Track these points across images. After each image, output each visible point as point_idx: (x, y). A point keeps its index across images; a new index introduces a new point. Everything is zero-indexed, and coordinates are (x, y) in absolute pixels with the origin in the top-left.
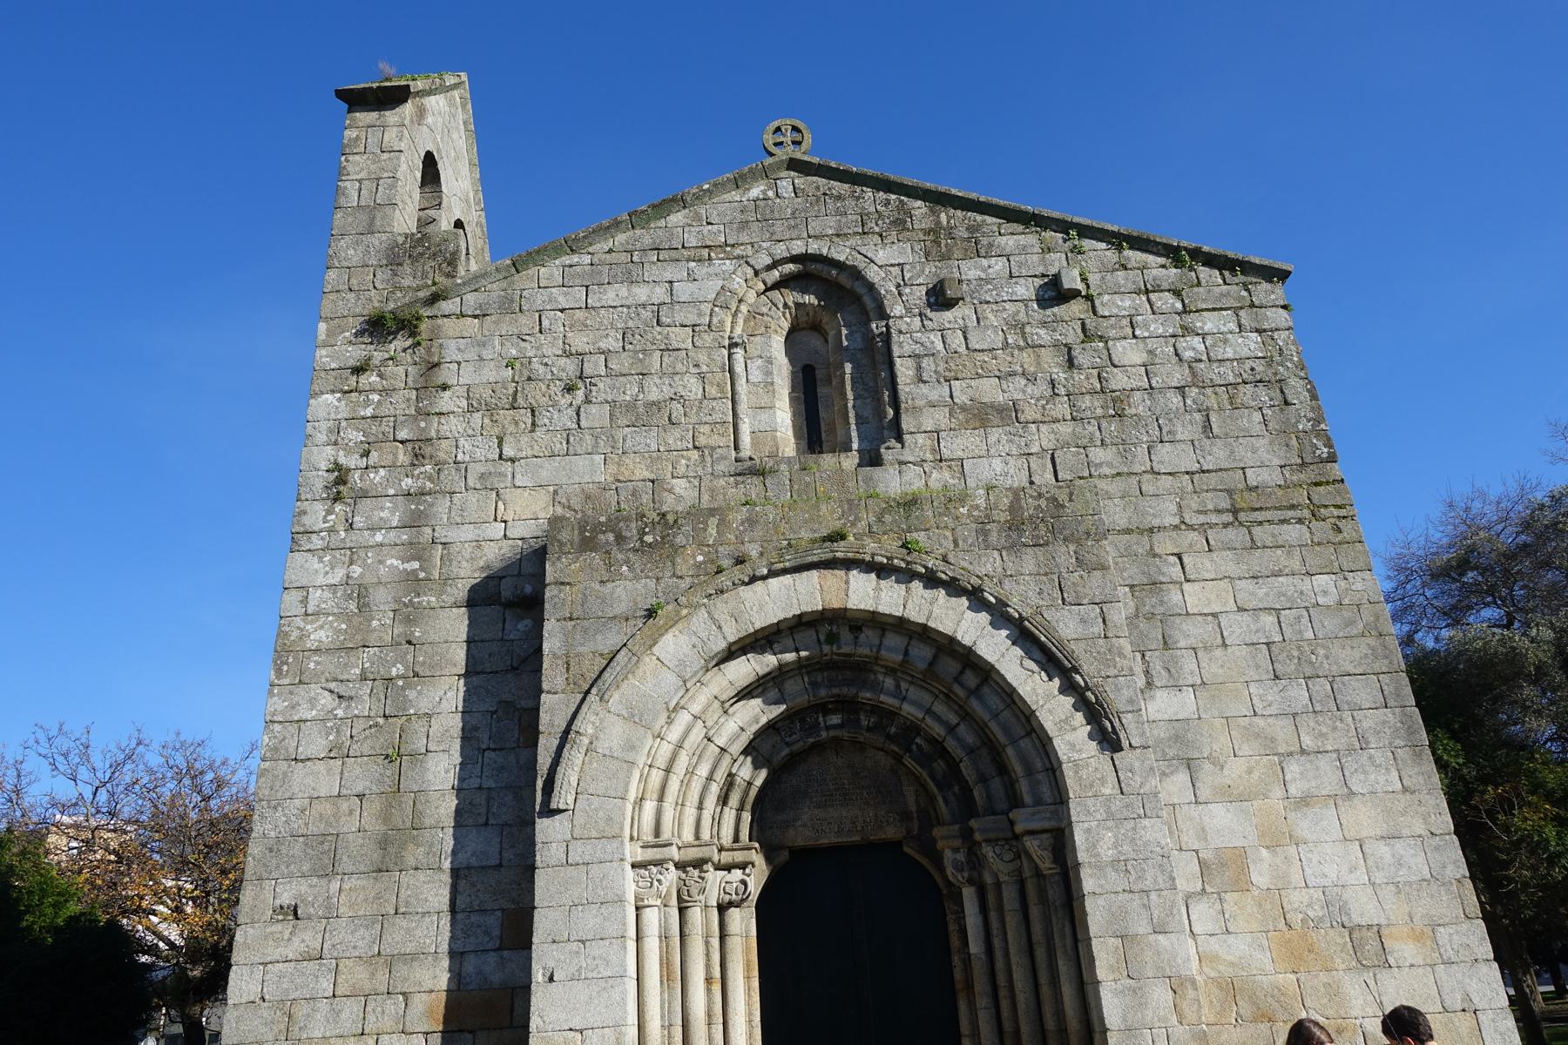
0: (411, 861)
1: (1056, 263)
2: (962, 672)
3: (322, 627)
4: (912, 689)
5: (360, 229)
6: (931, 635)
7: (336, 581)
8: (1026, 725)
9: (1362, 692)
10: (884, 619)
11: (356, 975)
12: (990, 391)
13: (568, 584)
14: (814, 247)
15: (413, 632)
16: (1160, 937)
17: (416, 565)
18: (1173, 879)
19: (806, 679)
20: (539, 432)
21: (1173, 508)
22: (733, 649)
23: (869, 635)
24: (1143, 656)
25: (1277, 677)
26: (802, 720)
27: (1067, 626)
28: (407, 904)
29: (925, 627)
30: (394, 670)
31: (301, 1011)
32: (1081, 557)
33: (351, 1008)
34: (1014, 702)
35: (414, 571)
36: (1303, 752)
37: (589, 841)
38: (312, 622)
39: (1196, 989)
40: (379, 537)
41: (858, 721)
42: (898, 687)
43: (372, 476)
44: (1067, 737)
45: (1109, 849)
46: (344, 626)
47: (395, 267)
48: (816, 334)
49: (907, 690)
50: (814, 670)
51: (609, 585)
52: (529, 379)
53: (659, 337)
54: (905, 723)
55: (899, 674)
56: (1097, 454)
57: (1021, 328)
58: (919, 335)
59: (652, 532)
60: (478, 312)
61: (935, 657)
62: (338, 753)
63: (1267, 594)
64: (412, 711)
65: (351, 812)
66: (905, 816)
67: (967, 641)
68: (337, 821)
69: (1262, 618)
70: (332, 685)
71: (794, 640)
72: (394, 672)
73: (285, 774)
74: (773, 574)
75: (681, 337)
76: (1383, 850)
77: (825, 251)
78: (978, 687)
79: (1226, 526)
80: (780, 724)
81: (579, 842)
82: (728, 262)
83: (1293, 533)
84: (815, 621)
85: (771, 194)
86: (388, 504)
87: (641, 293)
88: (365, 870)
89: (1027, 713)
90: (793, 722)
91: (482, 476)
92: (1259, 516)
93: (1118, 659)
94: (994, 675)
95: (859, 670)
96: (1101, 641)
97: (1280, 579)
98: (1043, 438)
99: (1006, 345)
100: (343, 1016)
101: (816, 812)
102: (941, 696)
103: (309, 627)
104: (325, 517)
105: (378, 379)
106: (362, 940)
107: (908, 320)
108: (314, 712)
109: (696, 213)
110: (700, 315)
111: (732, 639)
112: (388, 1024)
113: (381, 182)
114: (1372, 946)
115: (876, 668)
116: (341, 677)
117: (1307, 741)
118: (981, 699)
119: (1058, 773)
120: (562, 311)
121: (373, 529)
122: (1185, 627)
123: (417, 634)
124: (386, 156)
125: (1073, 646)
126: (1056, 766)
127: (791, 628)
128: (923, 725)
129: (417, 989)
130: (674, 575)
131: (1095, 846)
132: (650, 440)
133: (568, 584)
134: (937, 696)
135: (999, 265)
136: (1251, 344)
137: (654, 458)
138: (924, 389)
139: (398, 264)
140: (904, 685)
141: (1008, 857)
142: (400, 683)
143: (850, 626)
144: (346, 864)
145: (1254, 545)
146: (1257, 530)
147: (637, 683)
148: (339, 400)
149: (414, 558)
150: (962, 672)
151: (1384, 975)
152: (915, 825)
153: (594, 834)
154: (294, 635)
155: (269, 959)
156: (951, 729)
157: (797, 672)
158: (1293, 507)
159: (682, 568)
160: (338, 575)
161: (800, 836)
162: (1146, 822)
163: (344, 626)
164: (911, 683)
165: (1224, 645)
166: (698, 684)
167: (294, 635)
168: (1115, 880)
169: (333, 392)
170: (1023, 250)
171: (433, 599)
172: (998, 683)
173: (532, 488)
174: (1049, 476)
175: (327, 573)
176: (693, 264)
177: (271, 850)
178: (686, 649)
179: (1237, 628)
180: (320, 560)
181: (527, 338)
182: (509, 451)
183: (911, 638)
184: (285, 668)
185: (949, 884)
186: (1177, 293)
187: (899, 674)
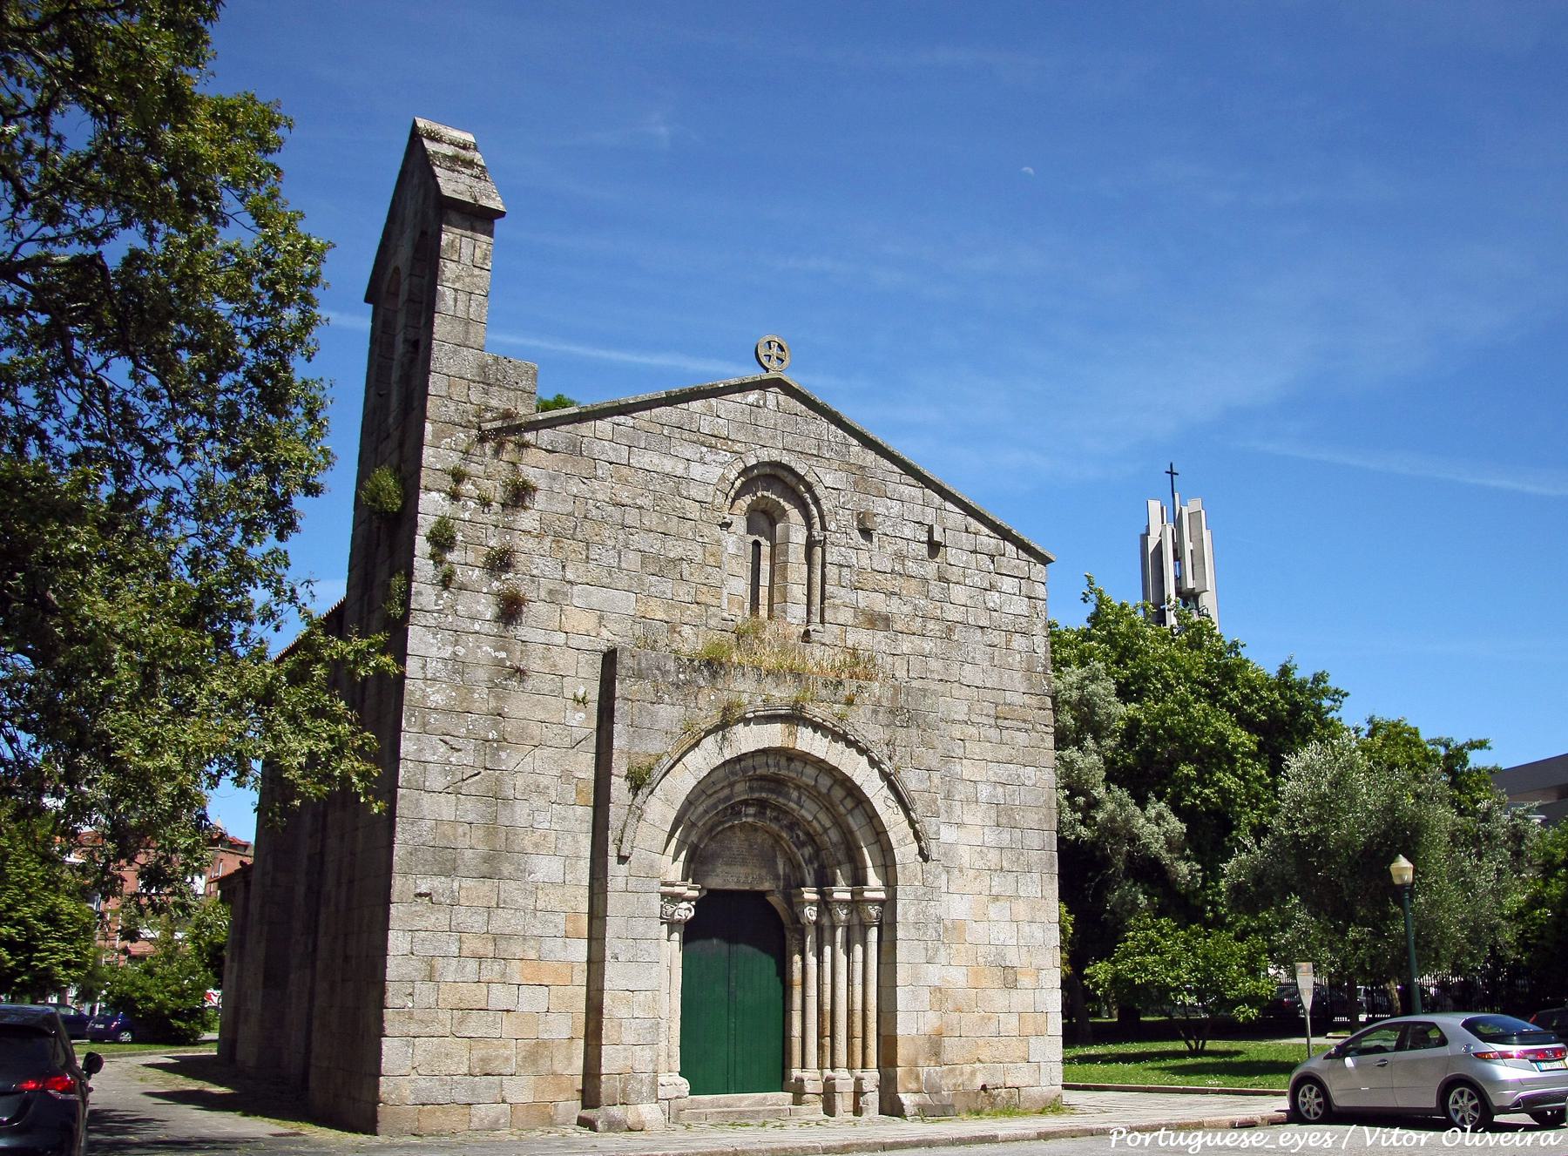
0: (506, 873)
1: (930, 517)
2: (845, 798)
3: (438, 691)
4: (808, 801)
5: (458, 341)
7: (447, 656)
9: (1034, 839)
11: (472, 944)
12: (879, 603)
14: (786, 459)
15: (503, 708)
17: (503, 655)
20: (592, 565)
21: (966, 709)
23: (797, 765)
27: (911, 781)
28: (505, 902)
31: (439, 963)
33: (472, 965)
38: (430, 686)
40: (477, 627)
41: (764, 814)
42: (800, 798)
43: (470, 573)
44: (902, 849)
46: (454, 694)
47: (485, 387)
48: (765, 517)
52: (586, 517)
53: (678, 506)
55: (802, 790)
56: (934, 664)
57: (900, 557)
58: (843, 549)
59: (684, 672)
60: (550, 448)
61: (832, 786)
62: (454, 790)
64: (504, 768)
66: (777, 877)
70: (447, 738)
72: (490, 737)
73: (417, 800)
75: (693, 510)
76: (1026, 929)
77: (793, 464)
78: (853, 809)
82: (728, 454)
83: (1021, 738)
85: (761, 403)
86: (483, 601)
87: (668, 465)
91: (550, 592)
92: (1007, 723)
95: (777, 784)
98: (906, 646)
99: (893, 572)
100: (468, 969)
103: (428, 690)
104: (436, 601)
105: (473, 488)
106: (477, 922)
107: (839, 535)
108: (436, 757)
109: (711, 406)
110: (707, 494)
112: (496, 977)
113: (473, 296)
114: (1010, 978)
116: (453, 733)
117: (1005, 864)
118: (852, 816)
120: (611, 463)
121: (473, 619)
122: (960, 787)
124: (477, 272)
132: (667, 587)
135: (896, 507)
136: (1021, 606)
137: (671, 603)
138: (843, 592)
139: (488, 384)
140: (803, 798)
142: (495, 745)
144: (462, 870)
148: (444, 499)
149: (503, 649)
150: (845, 798)
151: (1014, 992)
152: (782, 884)
154: (418, 693)
155: (415, 928)
156: (826, 830)
158: (1024, 721)
160: (447, 652)
161: (716, 882)
162: (932, 903)
163: (454, 694)
165: (977, 802)
167: (418, 693)
168: (913, 933)
169: (439, 491)
170: (912, 500)
173: (584, 609)
174: (905, 673)
175: (439, 648)
176: (704, 449)
177: (411, 854)
178: (701, 760)
179: (984, 792)
180: (435, 635)
181: (585, 480)
182: (570, 576)
184: (413, 719)
186: (992, 557)
187: (802, 790)
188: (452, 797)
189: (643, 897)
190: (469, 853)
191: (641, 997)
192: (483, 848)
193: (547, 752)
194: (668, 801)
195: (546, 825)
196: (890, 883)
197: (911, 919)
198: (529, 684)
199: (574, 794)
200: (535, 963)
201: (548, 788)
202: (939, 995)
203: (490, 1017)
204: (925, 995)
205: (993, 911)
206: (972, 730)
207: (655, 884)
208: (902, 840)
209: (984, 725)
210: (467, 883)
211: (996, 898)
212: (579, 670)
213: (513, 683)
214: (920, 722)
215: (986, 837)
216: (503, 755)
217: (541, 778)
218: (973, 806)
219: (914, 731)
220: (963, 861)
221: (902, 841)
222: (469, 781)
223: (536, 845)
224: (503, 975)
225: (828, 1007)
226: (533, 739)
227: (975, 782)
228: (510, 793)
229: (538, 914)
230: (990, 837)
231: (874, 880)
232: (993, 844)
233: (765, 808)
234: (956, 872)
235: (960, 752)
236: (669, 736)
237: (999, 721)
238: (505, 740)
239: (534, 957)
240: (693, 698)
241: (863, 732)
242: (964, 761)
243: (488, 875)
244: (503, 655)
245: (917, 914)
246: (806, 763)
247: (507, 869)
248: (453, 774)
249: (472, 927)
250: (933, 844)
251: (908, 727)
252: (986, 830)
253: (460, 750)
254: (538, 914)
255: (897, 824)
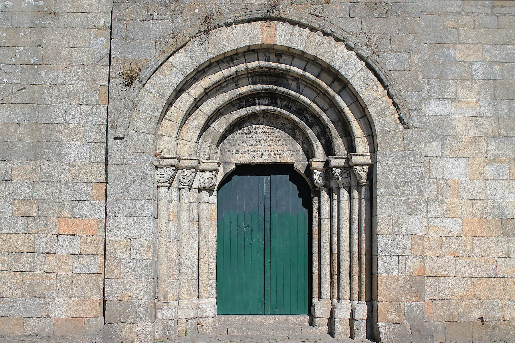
0: (46, 156)
2: (333, 82)
4: (306, 89)
6: (319, 62)
8: (362, 112)
10: (294, 51)
11: (21, 207)
13: (125, 20)
15: (42, 41)
16: (411, 217)
18: (422, 191)
19: (250, 80)
22: (212, 61)
24: (429, 81)
25: (495, 98)
26: (247, 101)
29: (315, 57)
30: (33, 60)
32: (404, 26)
34: (358, 100)
35: (41, 6)
36: (499, 135)
37: (134, 154)
39: (423, 240)
42: (298, 87)
44: (382, 120)
45: (393, 175)
46: (5, 35)
49: (303, 90)
50: (255, 75)
51: (147, 22)
54: (300, 106)
55: (300, 81)
63: (500, 54)
64: (43, 82)
65: (15, 131)
67: (337, 67)
68: (8, 135)
69: (495, 67)
71: (245, 59)
74: (237, 22)
79: (487, 15)
80: (235, 102)
81: (130, 154)
84: (257, 49)
88: (24, 159)
89: (364, 106)
90: (242, 102)
93: (414, 82)
94: (349, 86)
96: (407, 73)
97: (509, 47)
101: (251, 147)
102: (321, 94)
111: (211, 56)
115: (288, 77)
117: (502, 131)
119: (374, 137)
122: (453, 68)
123: (44, 41)
125: (392, 73)
126: (374, 134)
127: (244, 52)
128: (310, 108)
129: (51, 215)
130: (182, 19)
131: (387, 173)
133: (125, 20)
134: (319, 94)
140: (302, 87)
141: (345, 175)
143: (276, 53)
145: (498, 27)
146: (502, 19)
147: (161, 76)
153: (137, 150)
157: (245, 76)
159: (187, 15)
162: (414, 164)
163: (5, 35)
164: (306, 86)
165: (472, 79)
166: (193, 79)
171: (52, 23)
172: (350, 90)
178: (187, 60)
179: (479, 70)
183: (307, 63)
185: (315, 186)
188: (6, 106)
189: (137, 168)
190: (18, 144)
191: (138, 242)
192: (28, 140)
193: (76, 68)
194: (158, 94)
195: (76, 121)
196: (373, 150)
197: (392, 177)
198: (60, 23)
199: (97, 97)
200: (70, 219)
201: (77, 94)
202: (421, 242)
203: (36, 258)
204: (407, 242)
205: (490, 172)
206: (468, 19)
207: (150, 157)
208: (383, 112)
209: (479, 14)
210: (17, 165)
211: (493, 160)
212: (101, 6)
213: (49, 22)
214: (399, 12)
215: (482, 109)
216: (43, 74)
217: (71, 88)
218: (468, 83)
219: (392, 20)
220: (457, 130)
221: (382, 114)
222: (18, 94)
223: (69, 135)
224: (45, 228)
225: (335, 251)
226: (65, 60)
227: (470, 63)
228: (49, 100)
229: (71, 184)
230: (485, 108)
231: (339, 144)
232: (489, 114)
233: (276, 99)
234: (450, 139)
235: (453, 38)
236: (158, 43)
237: (496, 10)
238: (44, 63)
239: (68, 215)
240: (179, 13)
241: (341, 25)
242: (458, 46)
243: (32, 159)
244: (41, 3)
245: (398, 174)
246: (294, 57)
247: (46, 153)
248: (6, 90)
249: (21, 195)
250: (414, 114)
251: (386, 17)
252: (482, 103)
253: (10, 73)
254: (71, 184)
255: (376, 99)
